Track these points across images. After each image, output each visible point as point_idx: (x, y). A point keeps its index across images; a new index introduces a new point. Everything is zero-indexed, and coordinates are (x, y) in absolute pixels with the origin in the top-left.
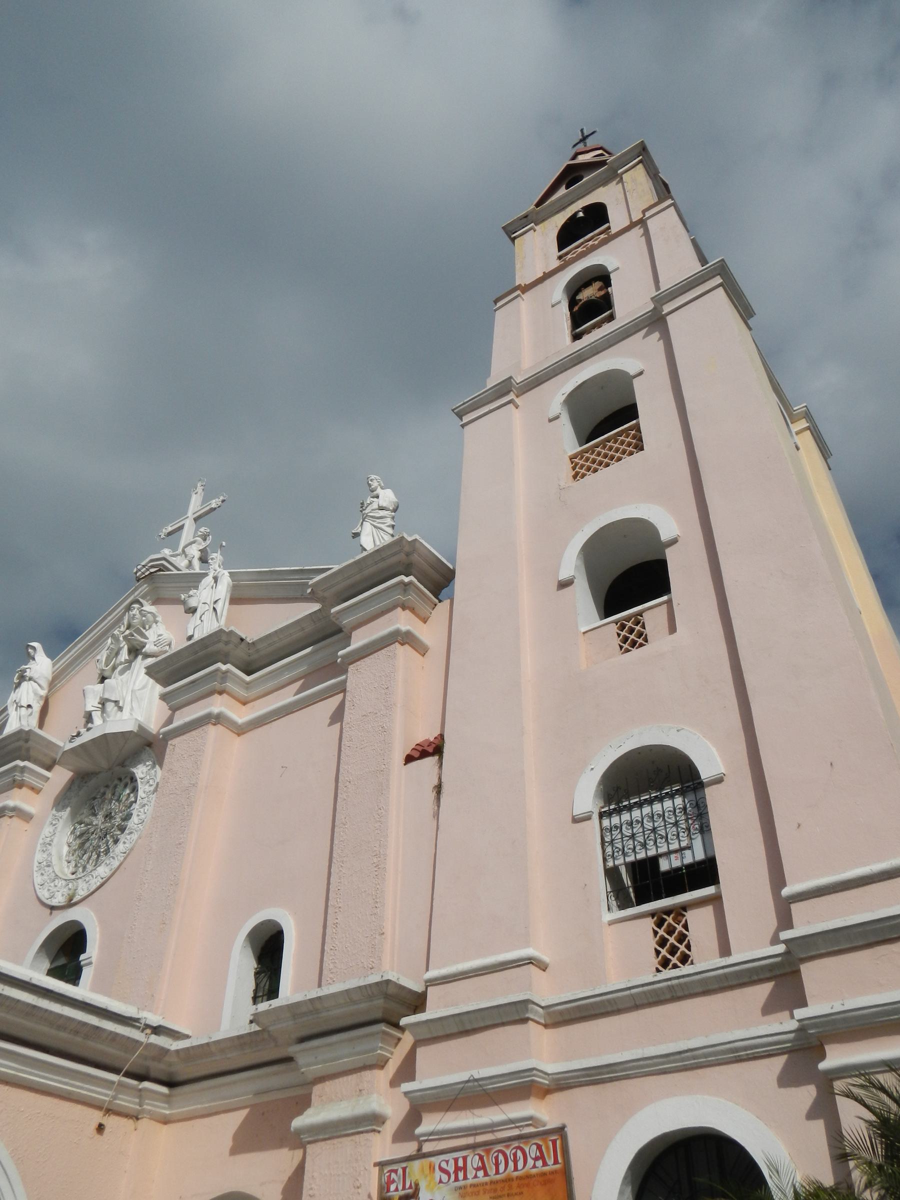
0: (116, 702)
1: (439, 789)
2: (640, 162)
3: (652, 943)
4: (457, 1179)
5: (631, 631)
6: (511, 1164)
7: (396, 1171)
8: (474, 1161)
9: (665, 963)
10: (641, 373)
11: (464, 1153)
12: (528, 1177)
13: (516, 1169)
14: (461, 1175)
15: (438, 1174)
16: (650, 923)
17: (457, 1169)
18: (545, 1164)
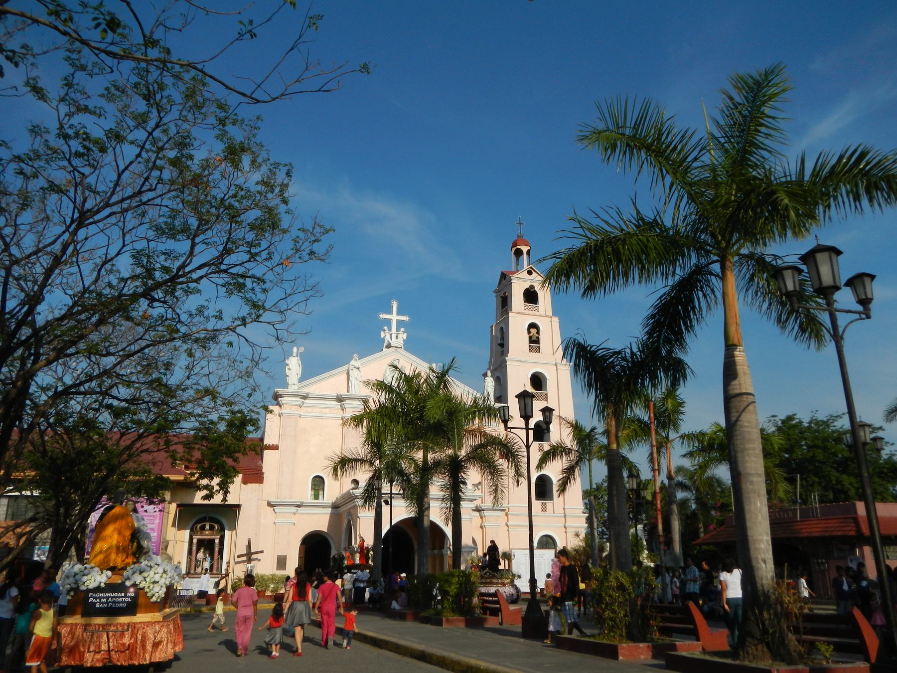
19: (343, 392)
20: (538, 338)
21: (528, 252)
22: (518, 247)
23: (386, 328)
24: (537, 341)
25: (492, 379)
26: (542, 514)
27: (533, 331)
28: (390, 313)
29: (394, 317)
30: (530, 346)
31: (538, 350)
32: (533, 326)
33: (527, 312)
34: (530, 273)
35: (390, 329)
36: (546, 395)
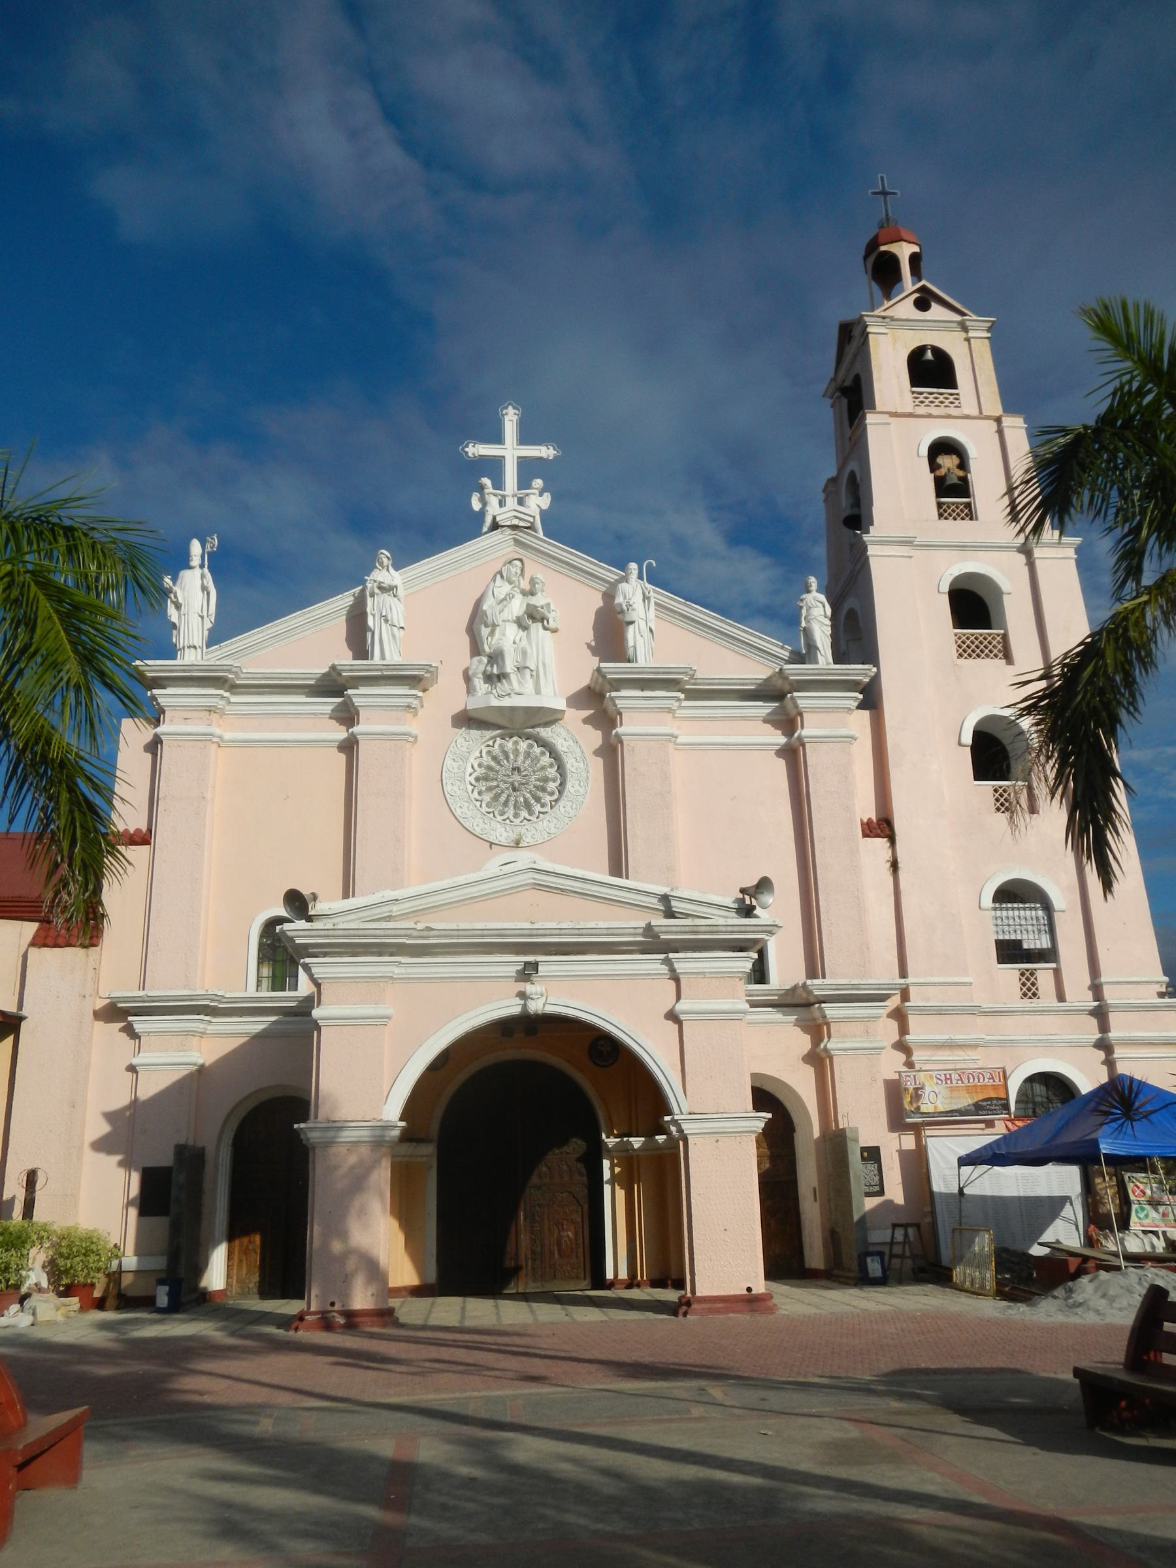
0: (531, 670)
1: (895, 865)
2: (988, 338)
3: (1019, 985)
4: (946, 1083)
5: (1001, 795)
6: (976, 1080)
7: (909, 1076)
8: (955, 1077)
9: (1025, 995)
10: (1009, 594)
11: (950, 1072)
12: (976, 1086)
13: (979, 1082)
14: (949, 1082)
15: (935, 1080)
16: (1017, 973)
17: (946, 1079)
18: (994, 1081)
19: (344, 658)
20: (964, 480)
21: (915, 259)
22: (883, 248)
23: (486, 481)
24: (961, 488)
25: (822, 598)
26: (1027, 1003)
27: (948, 462)
28: (498, 439)
29: (510, 451)
30: (939, 505)
31: (969, 513)
32: (942, 448)
33: (922, 410)
34: (922, 304)
35: (499, 484)
36: (1005, 637)
